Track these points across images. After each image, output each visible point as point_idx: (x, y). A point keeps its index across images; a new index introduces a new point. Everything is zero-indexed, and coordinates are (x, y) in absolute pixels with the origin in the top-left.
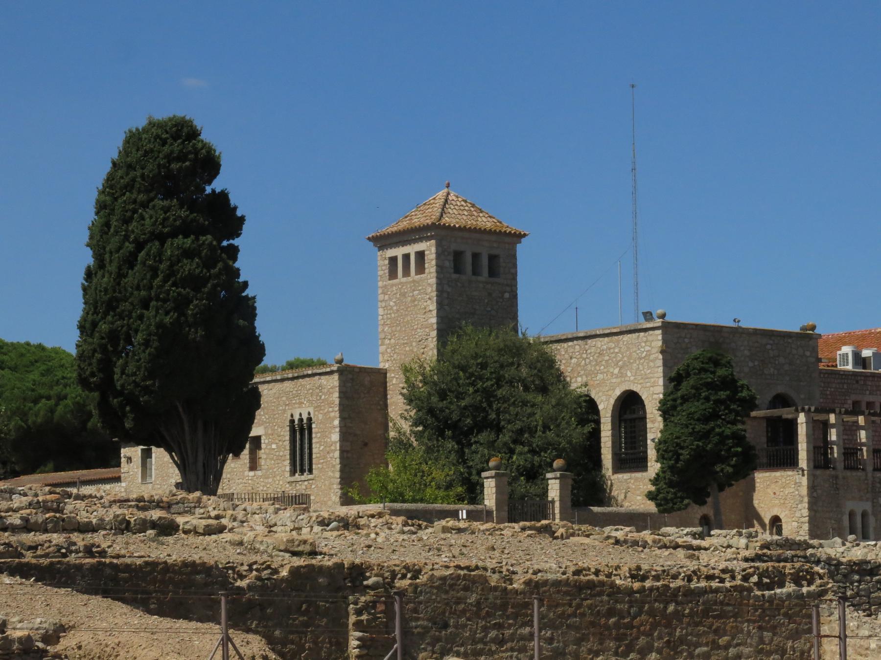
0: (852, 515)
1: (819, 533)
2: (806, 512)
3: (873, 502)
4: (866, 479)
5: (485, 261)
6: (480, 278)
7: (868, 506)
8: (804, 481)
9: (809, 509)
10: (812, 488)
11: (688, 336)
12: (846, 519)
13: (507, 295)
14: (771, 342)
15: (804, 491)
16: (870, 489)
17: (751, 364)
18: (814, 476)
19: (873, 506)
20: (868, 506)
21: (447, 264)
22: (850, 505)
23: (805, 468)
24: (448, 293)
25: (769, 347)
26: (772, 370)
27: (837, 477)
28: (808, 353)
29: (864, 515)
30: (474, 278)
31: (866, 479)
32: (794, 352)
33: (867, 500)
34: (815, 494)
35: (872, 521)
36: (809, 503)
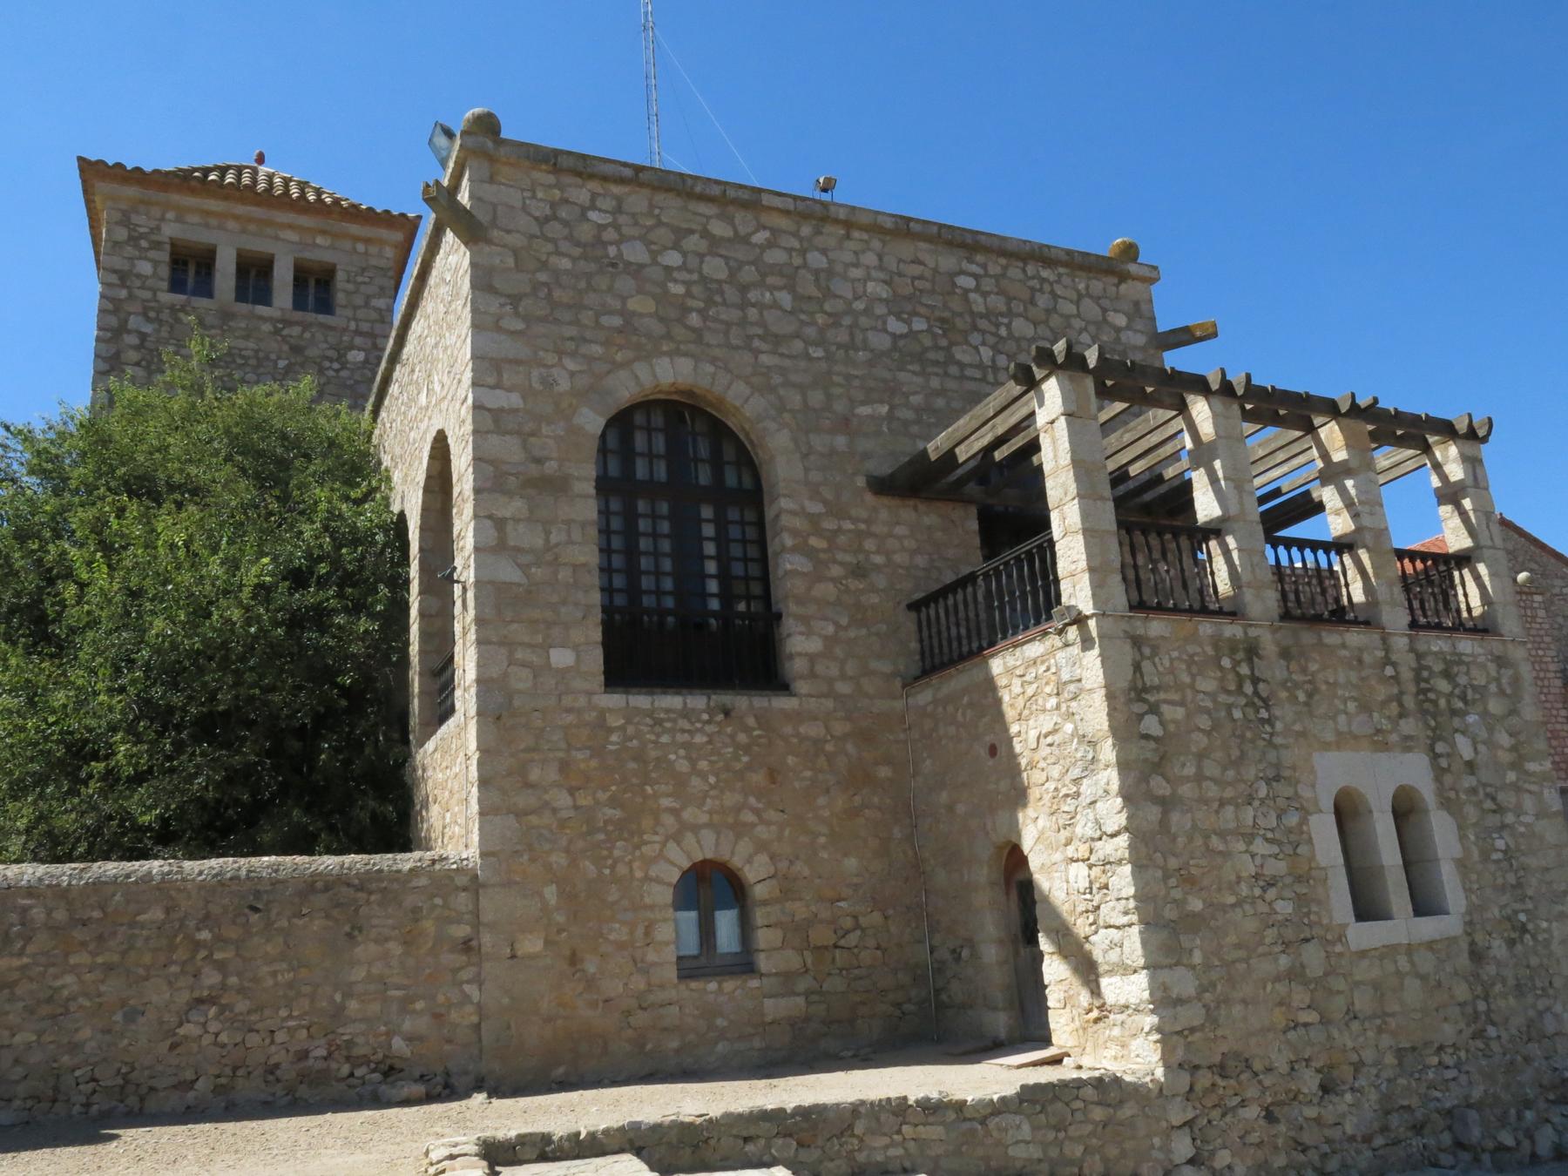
0: (1347, 812)
1: (1196, 905)
2: (1113, 813)
3: (1435, 757)
4: (1387, 661)
5: (283, 276)
6: (261, 310)
7: (1414, 771)
8: (1091, 668)
9: (1129, 797)
10: (1132, 700)
11: (607, 204)
12: (1324, 830)
13: (357, 356)
14: (974, 268)
15: (1095, 714)
16: (1409, 701)
17: (895, 326)
18: (1137, 642)
19: (1439, 773)
20: (1414, 771)
21: (145, 268)
22: (1333, 770)
23: (1087, 608)
24: (143, 337)
25: (968, 282)
26: (986, 353)
27: (1252, 651)
28: (1121, 320)
29: (1405, 810)
30: (244, 308)
31: (1387, 661)
32: (1068, 308)
33: (1407, 743)
34: (1151, 725)
35: (1442, 832)
36: (1123, 766)
